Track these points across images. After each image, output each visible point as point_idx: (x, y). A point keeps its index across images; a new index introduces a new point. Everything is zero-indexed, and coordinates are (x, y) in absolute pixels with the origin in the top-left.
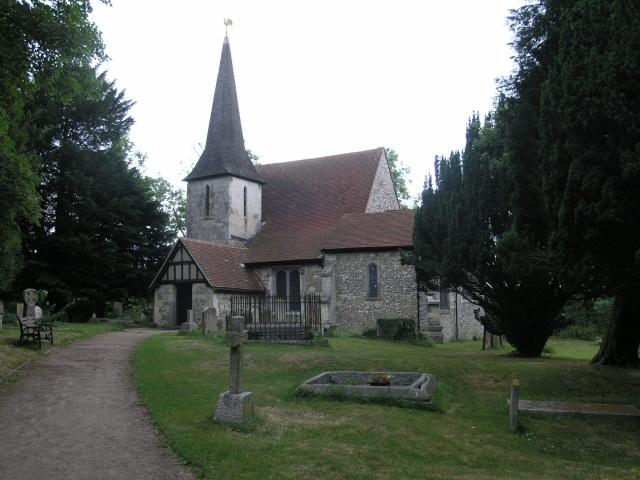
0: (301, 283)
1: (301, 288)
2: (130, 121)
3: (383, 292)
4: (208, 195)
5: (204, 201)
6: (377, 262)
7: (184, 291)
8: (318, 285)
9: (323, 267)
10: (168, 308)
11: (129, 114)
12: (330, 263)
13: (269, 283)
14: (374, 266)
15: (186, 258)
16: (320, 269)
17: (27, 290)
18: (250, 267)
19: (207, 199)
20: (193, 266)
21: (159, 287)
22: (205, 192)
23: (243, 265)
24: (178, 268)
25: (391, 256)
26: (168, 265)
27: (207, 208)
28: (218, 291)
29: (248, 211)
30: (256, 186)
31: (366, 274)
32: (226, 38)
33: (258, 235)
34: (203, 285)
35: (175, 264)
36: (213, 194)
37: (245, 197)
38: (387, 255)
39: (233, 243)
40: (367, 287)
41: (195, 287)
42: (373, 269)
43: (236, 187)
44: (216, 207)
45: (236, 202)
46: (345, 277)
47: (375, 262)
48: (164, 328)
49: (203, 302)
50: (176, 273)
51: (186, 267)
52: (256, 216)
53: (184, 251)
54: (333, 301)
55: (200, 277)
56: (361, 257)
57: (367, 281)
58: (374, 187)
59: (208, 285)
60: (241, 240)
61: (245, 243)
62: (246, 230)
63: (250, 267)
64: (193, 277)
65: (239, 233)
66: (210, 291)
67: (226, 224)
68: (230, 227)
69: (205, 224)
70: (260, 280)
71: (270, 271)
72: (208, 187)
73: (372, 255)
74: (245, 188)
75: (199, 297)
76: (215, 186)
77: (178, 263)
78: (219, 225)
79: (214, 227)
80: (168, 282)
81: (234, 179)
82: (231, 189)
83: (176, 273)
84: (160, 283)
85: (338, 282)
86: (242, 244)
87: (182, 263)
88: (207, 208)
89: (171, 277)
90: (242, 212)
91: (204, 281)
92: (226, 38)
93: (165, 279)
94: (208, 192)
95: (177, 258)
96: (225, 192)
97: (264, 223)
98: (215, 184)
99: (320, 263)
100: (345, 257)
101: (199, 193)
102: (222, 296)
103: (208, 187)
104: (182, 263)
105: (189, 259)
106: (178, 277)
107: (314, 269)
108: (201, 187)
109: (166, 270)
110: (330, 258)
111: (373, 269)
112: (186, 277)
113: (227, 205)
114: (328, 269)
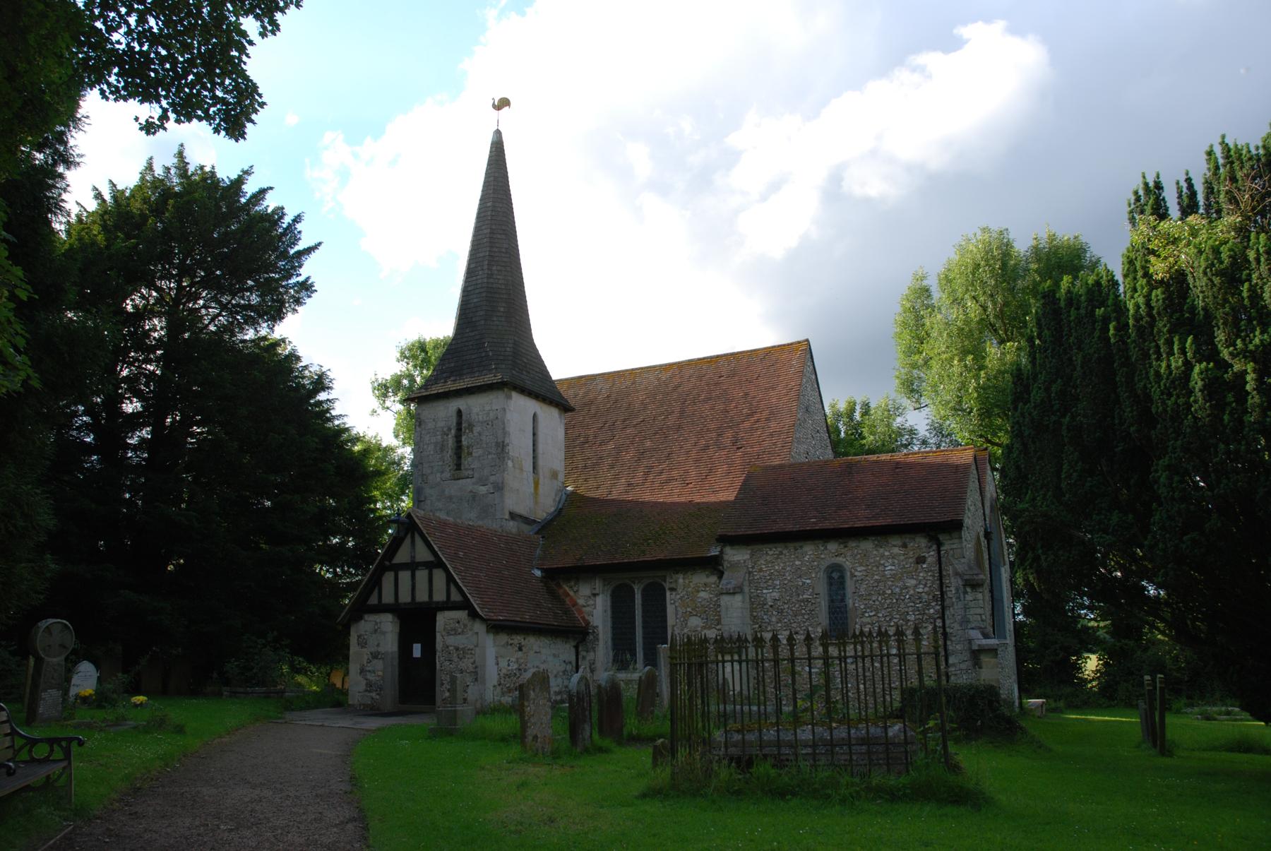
0: (670, 609)
1: (671, 620)
2: (306, 287)
4: (459, 429)
5: (451, 442)
6: (846, 562)
7: (417, 622)
8: (713, 614)
9: (721, 575)
10: (378, 664)
11: (308, 269)
12: (734, 566)
13: (595, 605)
15: (423, 554)
16: (713, 579)
17: (43, 624)
18: (554, 576)
20: (439, 576)
21: (361, 618)
23: (538, 573)
24: (405, 576)
26: (381, 570)
27: (459, 457)
28: (496, 628)
29: (541, 463)
30: (554, 413)
31: (822, 588)
32: (498, 133)
33: (559, 512)
34: (462, 615)
35: (397, 568)
36: (471, 427)
37: (534, 434)
38: (867, 545)
39: (512, 526)
40: (823, 619)
41: (443, 619)
42: (836, 578)
44: (477, 452)
45: (519, 444)
46: (771, 595)
47: (840, 560)
48: (373, 711)
49: (462, 652)
50: (402, 587)
51: (422, 575)
55: (456, 597)
56: (809, 550)
57: (823, 603)
59: (474, 615)
62: (536, 503)
63: (554, 576)
64: (439, 596)
65: (521, 510)
66: (479, 627)
67: (499, 488)
69: (453, 488)
70: (575, 604)
71: (598, 584)
72: (459, 412)
73: (833, 546)
74: (535, 416)
75: (451, 640)
76: (475, 410)
78: (483, 490)
79: (474, 496)
80: (381, 609)
81: (514, 395)
82: (508, 416)
83: (402, 587)
84: (361, 609)
85: (756, 604)
87: (413, 566)
89: (388, 598)
90: (528, 466)
91: (465, 605)
92: (498, 133)
93: (373, 600)
94: (459, 424)
95: (402, 556)
96: (497, 423)
98: (476, 406)
99: (714, 565)
100: (771, 552)
101: (441, 424)
102: (503, 638)
103: (459, 412)
104: (413, 566)
105: (431, 558)
106: (405, 597)
107: (700, 578)
108: (444, 412)
109: (375, 582)
110: (736, 555)
111: (836, 578)
112: (422, 596)
113: (502, 447)
114: (730, 580)
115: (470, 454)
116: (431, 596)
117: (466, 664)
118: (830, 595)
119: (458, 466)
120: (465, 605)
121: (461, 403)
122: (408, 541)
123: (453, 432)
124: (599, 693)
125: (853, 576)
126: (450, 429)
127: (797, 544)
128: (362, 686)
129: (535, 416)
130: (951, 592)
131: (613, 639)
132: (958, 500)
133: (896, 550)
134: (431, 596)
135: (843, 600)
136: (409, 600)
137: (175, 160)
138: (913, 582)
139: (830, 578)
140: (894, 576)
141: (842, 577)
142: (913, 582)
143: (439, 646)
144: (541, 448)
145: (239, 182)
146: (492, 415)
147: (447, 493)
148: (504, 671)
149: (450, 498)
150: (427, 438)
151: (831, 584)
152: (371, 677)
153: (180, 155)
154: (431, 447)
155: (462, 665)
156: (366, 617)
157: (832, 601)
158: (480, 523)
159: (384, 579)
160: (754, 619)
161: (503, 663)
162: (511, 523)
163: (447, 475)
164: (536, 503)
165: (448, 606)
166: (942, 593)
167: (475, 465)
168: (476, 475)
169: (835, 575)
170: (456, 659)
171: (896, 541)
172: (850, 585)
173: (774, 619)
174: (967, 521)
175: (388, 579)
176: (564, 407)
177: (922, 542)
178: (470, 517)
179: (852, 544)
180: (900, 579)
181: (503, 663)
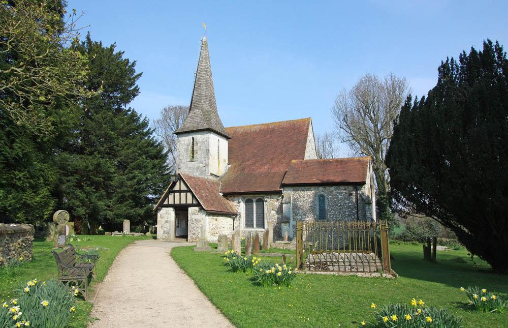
3: (328, 215)
4: (193, 144)
5: (190, 148)
7: (181, 211)
14: (323, 196)
15: (184, 188)
19: (193, 148)
22: (192, 140)
23: (221, 194)
24: (177, 195)
25: (336, 189)
27: (193, 154)
29: (220, 158)
34: (197, 208)
36: (197, 143)
38: (333, 188)
39: (211, 178)
41: (190, 209)
43: (213, 138)
44: (199, 152)
47: (323, 193)
51: (183, 194)
52: (225, 161)
53: (182, 183)
54: (291, 221)
57: (318, 208)
58: (308, 143)
59: (202, 209)
60: (216, 176)
61: (219, 178)
62: (219, 171)
64: (190, 202)
67: (207, 165)
68: (209, 166)
69: (191, 164)
72: (193, 138)
73: (321, 188)
74: (218, 140)
75: (193, 217)
77: (177, 191)
79: (198, 167)
80: (168, 206)
84: (162, 206)
86: (216, 179)
87: (180, 191)
88: (193, 154)
89: (171, 202)
91: (199, 205)
93: (166, 203)
94: (193, 142)
95: (177, 188)
96: (206, 143)
97: (229, 166)
98: (199, 137)
101: (186, 142)
103: (193, 138)
104: (180, 191)
106: (177, 202)
107: (276, 197)
109: (167, 196)
112: (183, 202)
113: (208, 151)
115: (197, 153)
116: (186, 202)
117: (199, 225)
118: (320, 205)
119: (193, 157)
120: (199, 205)
121: (194, 136)
122: (178, 183)
123: (191, 145)
124: (253, 236)
125: (327, 198)
126: (190, 144)
127: (309, 187)
128: (162, 232)
129: (218, 140)
130: (360, 206)
131: (246, 217)
132: (365, 175)
133: (342, 191)
134: (186, 202)
135: (324, 207)
136: (179, 203)
137: (86, 40)
138: (348, 202)
139: (319, 199)
140: (341, 199)
141: (324, 199)
142: (348, 202)
143: (189, 219)
144: (220, 152)
145: (111, 50)
146: (205, 140)
147: (189, 165)
148: (211, 228)
149: (190, 168)
150: (181, 147)
151: (320, 201)
152: (165, 229)
153: (88, 38)
154: (183, 150)
155: (197, 225)
156: (163, 208)
157: (320, 207)
158: (201, 176)
159: (170, 196)
160: (294, 212)
161: (211, 225)
162: (211, 177)
163: (189, 160)
164: (219, 171)
165: (192, 205)
166: (358, 206)
167: (199, 157)
168: (199, 160)
169: (321, 198)
170: (195, 223)
171: (343, 187)
172: (326, 202)
173: (300, 212)
174: (367, 182)
175: (171, 197)
176: (227, 138)
177: (351, 188)
178: (197, 174)
179: (327, 188)
180: (343, 201)
181: (211, 225)
